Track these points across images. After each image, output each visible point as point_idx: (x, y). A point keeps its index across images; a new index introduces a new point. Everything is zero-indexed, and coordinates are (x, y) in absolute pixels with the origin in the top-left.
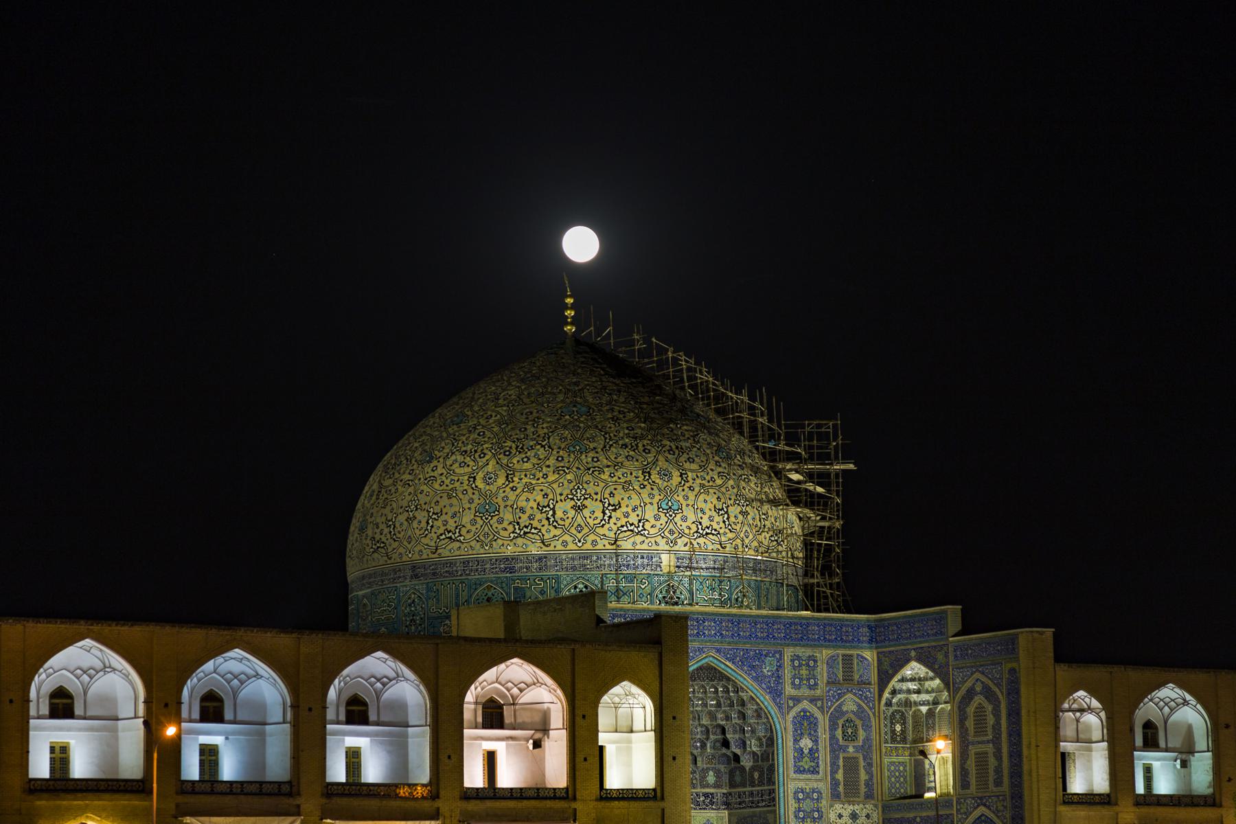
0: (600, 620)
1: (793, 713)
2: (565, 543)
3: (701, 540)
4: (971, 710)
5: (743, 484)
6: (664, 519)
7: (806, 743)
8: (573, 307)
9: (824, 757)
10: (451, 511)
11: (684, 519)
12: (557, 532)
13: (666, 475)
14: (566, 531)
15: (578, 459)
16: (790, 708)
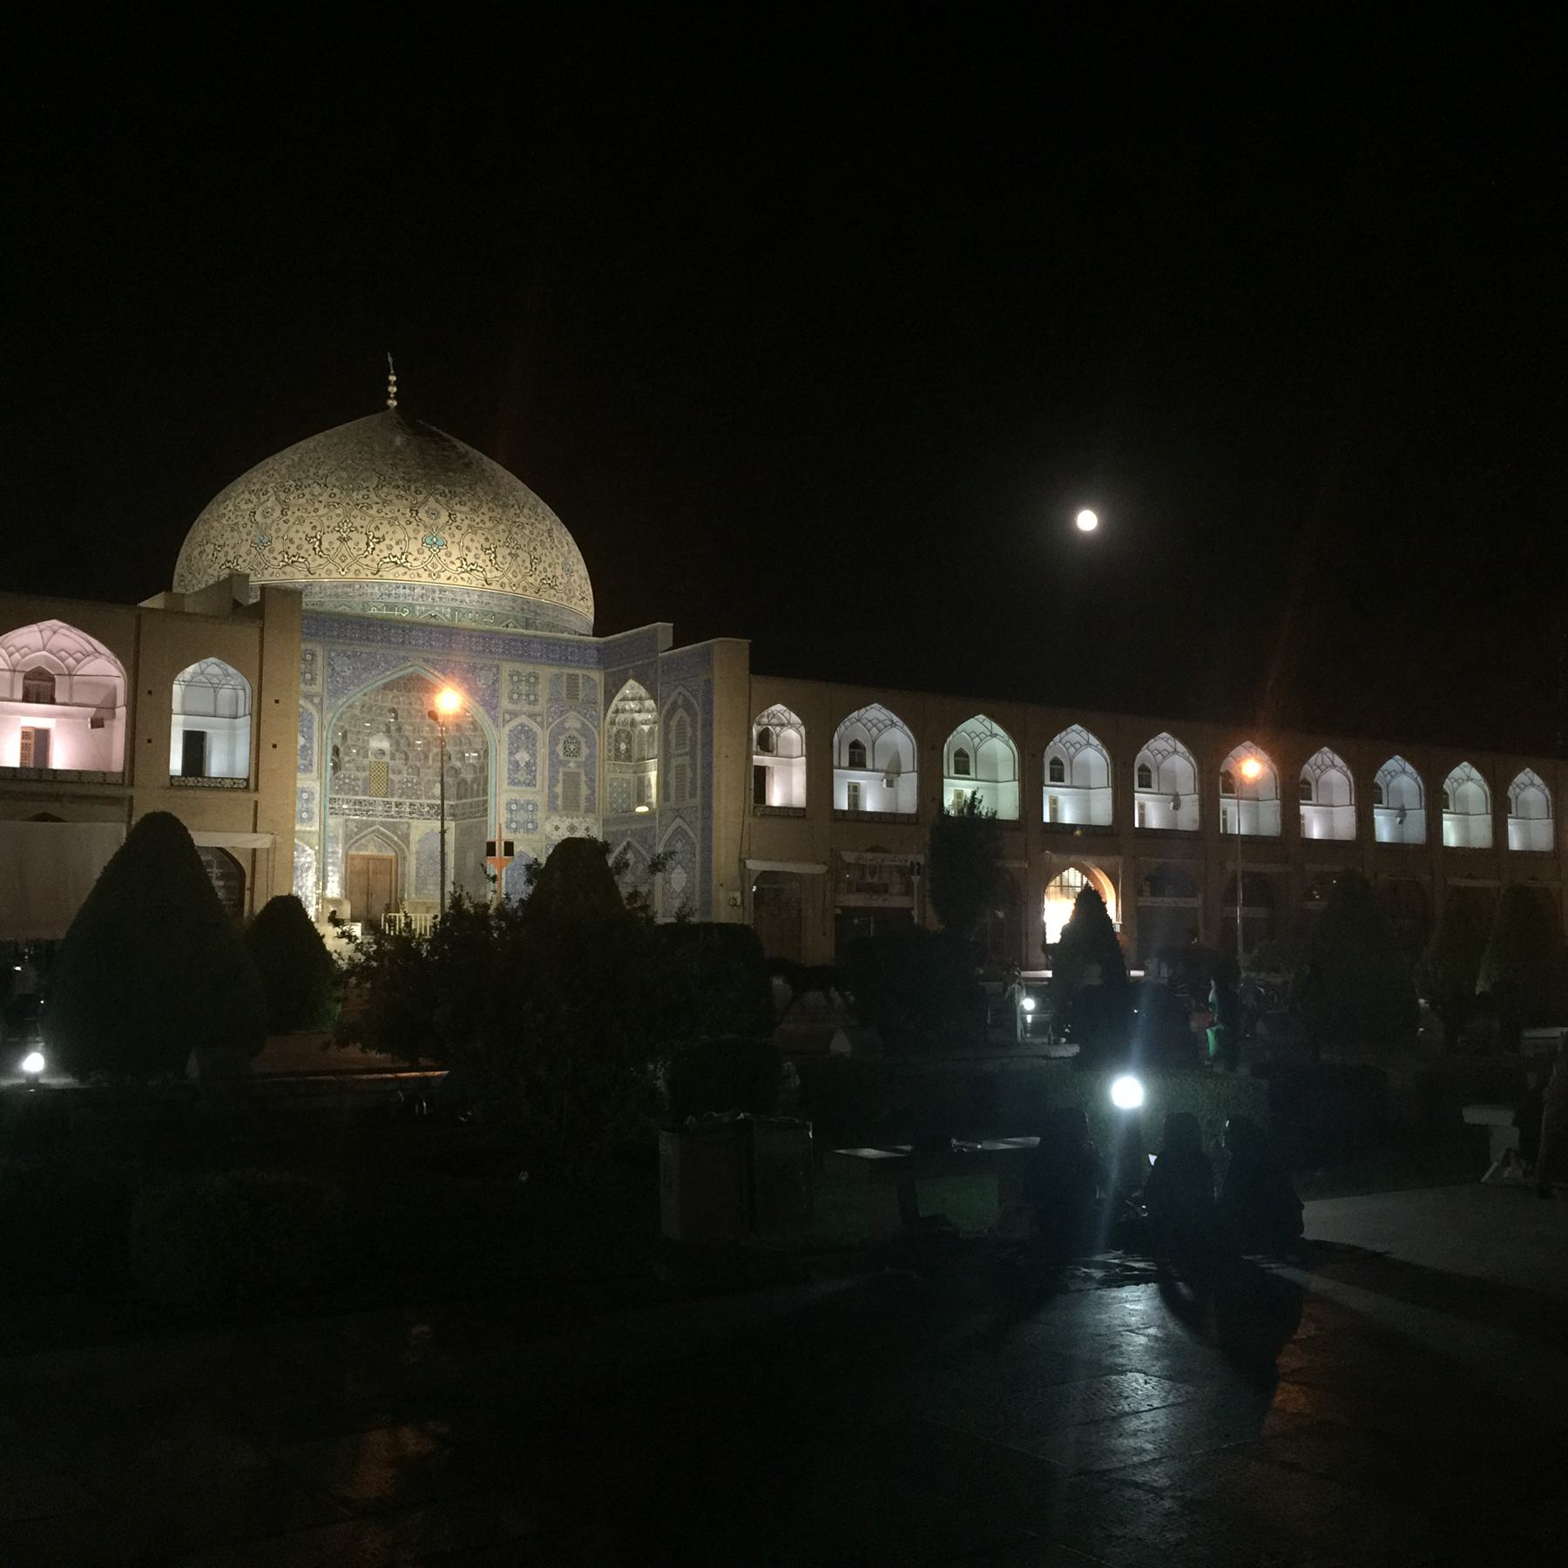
0: (237, 605)
1: (509, 727)
2: (329, 572)
3: (465, 576)
4: (673, 723)
5: (515, 530)
6: (427, 554)
7: (523, 757)
8: (396, 383)
9: (543, 771)
10: (231, 542)
11: (449, 555)
12: (322, 561)
13: (434, 514)
14: (330, 560)
15: (348, 495)
16: (505, 722)
